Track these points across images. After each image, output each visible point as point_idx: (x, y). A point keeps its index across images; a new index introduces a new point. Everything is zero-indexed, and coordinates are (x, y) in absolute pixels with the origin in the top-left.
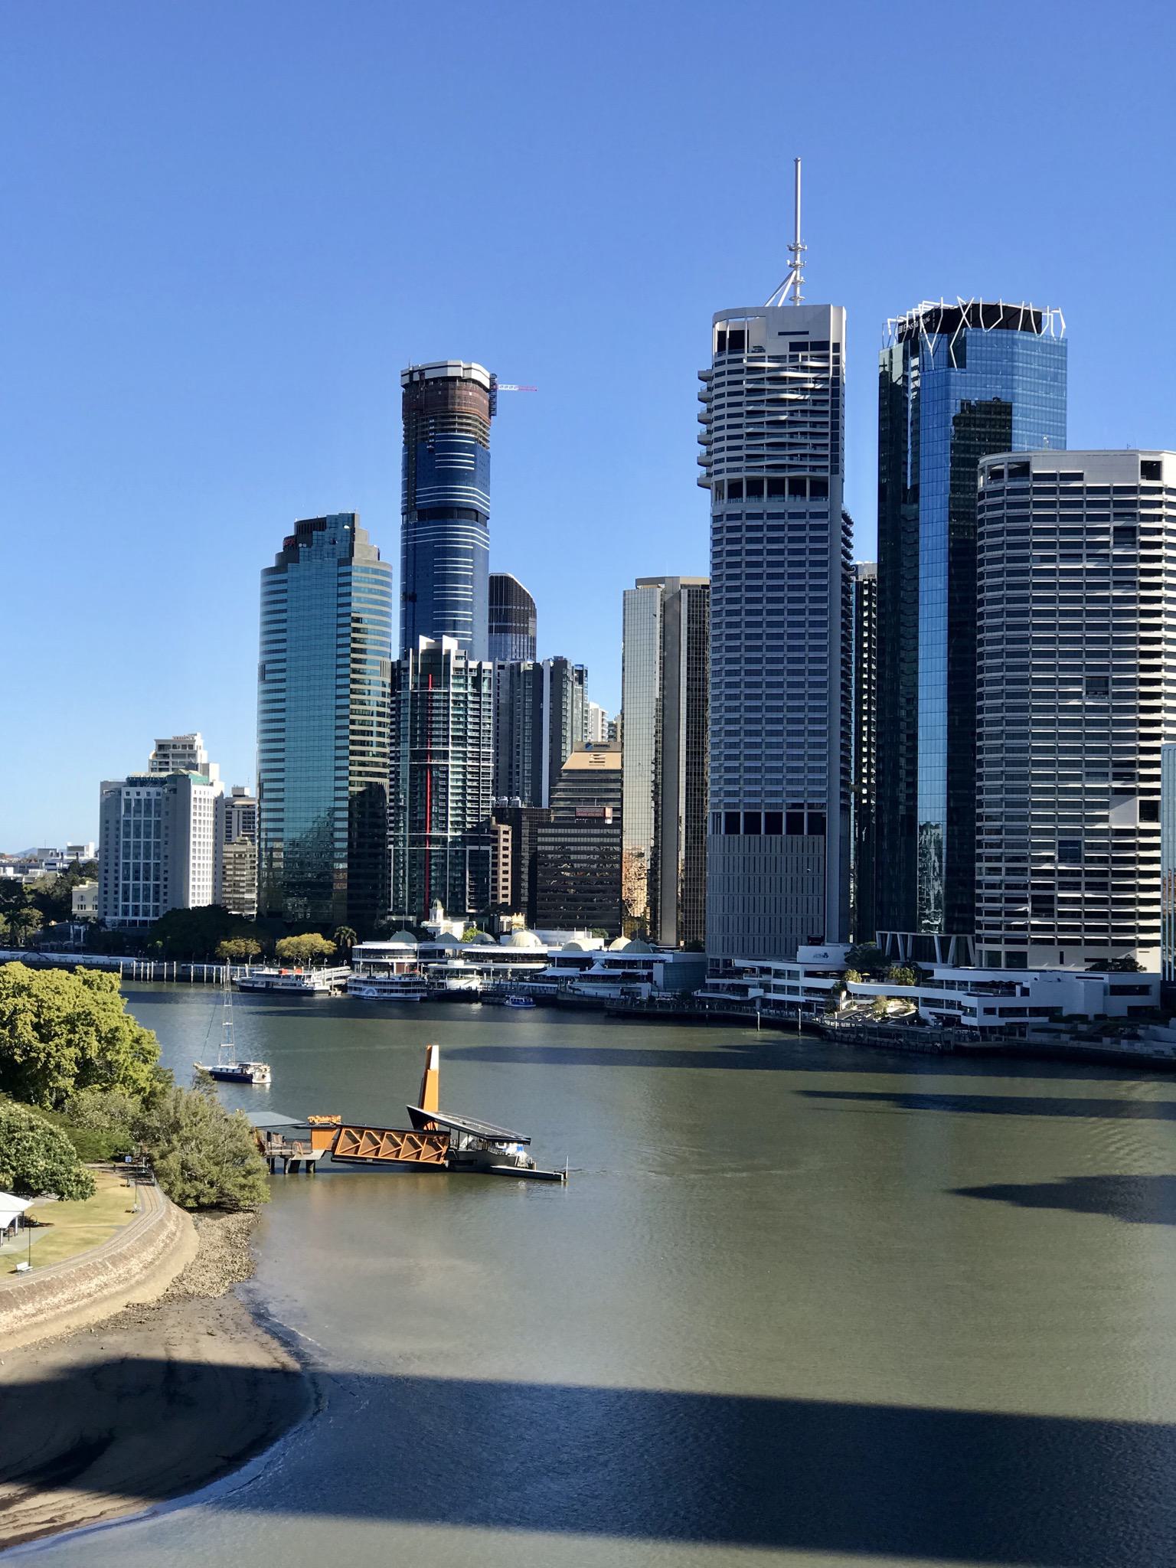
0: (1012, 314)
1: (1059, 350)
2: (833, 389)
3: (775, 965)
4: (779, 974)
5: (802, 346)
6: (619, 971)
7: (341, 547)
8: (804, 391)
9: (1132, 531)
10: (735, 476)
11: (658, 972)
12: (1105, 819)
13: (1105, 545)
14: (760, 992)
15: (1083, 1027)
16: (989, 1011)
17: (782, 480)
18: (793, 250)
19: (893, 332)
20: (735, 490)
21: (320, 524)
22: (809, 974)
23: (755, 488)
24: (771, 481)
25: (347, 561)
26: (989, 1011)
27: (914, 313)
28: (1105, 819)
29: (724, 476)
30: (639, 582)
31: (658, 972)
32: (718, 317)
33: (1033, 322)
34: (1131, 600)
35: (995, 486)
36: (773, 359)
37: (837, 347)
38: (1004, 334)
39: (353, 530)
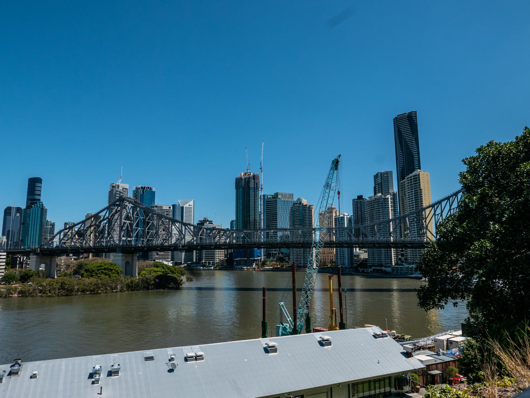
0: (150, 188)
1: (154, 192)
5: (124, 189)
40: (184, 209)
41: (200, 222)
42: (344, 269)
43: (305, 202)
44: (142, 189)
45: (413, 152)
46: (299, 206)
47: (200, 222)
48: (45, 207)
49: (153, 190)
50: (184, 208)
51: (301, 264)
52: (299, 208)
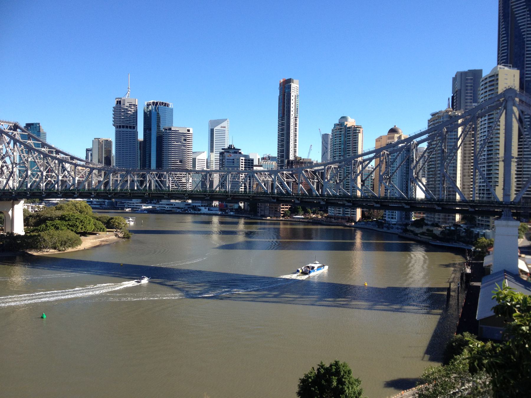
0: (166, 104)
1: (172, 110)
2: (136, 112)
3: (130, 202)
4: (130, 203)
5: (131, 105)
6: (99, 203)
7: (38, 128)
8: (132, 112)
9: (186, 139)
10: (120, 125)
11: (106, 203)
12: (182, 181)
13: (182, 141)
14: (127, 206)
15: (183, 210)
16: (170, 208)
17: (128, 126)
18: (128, 88)
19: (146, 104)
20: (120, 127)
21: (32, 124)
22: (136, 203)
23: (123, 127)
24: (126, 126)
25: (40, 131)
26: (170, 208)
27: (150, 102)
28: (182, 181)
29: (118, 125)
30: (95, 139)
31: (106, 203)
32: (116, 99)
33: (168, 105)
34: (186, 149)
35: (166, 131)
36: (126, 106)
37: (137, 105)
38: (164, 107)
39: (39, 126)
40: (215, 132)
41: (224, 151)
42: (391, 225)
43: (350, 122)
44: (153, 105)
45: (524, 35)
46: (340, 129)
47: (224, 151)
48: (43, 130)
49: (170, 106)
50: (215, 131)
51: (340, 213)
52: (340, 132)
